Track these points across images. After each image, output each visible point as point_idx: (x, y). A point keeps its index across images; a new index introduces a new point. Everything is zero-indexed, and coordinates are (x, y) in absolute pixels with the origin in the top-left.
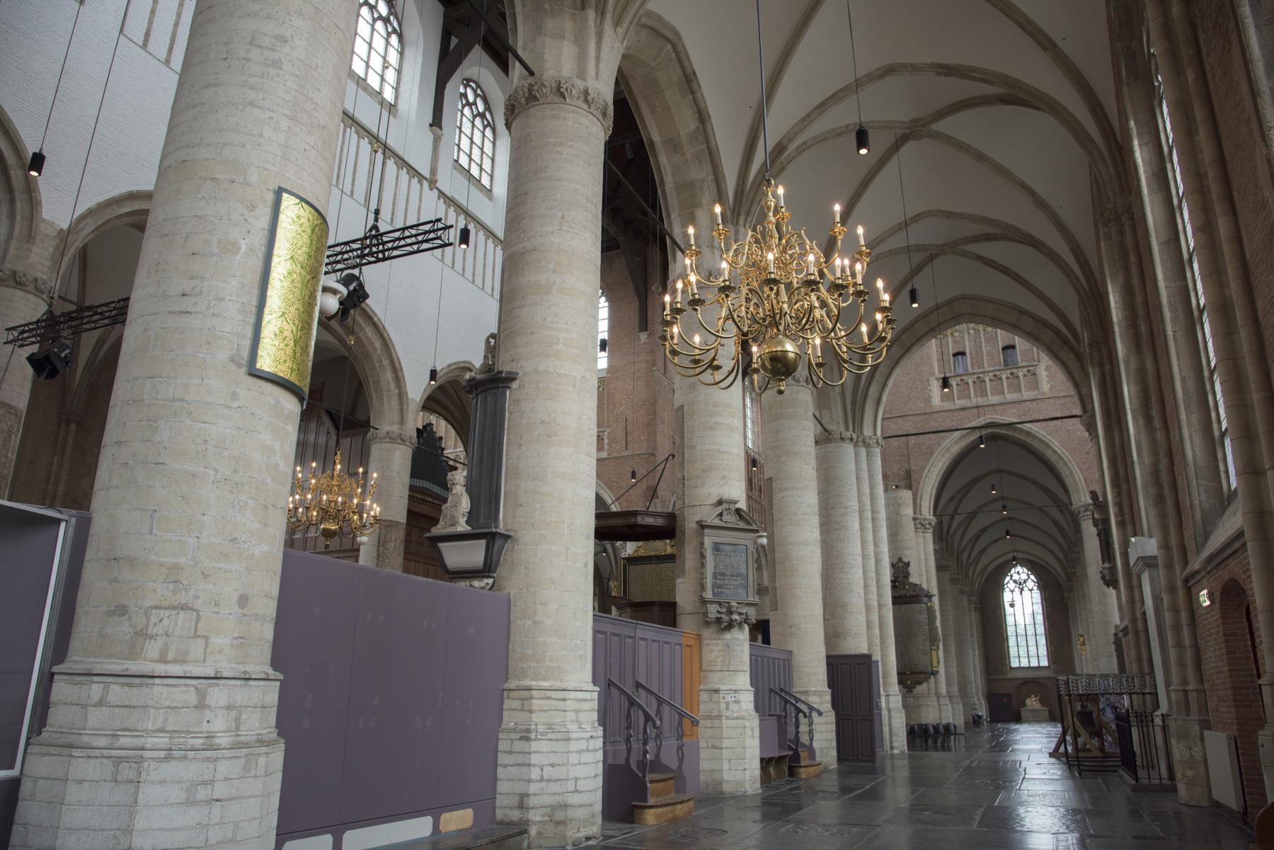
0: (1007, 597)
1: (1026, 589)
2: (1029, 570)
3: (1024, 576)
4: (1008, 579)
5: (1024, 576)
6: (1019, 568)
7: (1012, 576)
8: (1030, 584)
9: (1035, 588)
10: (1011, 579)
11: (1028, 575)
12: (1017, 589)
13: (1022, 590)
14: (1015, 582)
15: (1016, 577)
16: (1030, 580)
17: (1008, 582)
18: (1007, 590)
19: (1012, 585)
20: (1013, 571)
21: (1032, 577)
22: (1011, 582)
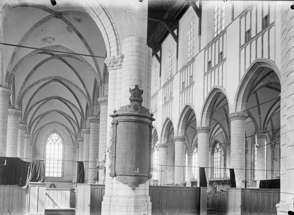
0: (48, 146)
1: (57, 143)
2: (59, 136)
4: (49, 138)
5: (57, 138)
6: (55, 135)
7: (51, 137)
8: (59, 142)
9: (61, 143)
11: (58, 138)
12: (53, 143)
13: (55, 144)
14: (52, 140)
16: (59, 140)
17: (49, 140)
18: (48, 143)
20: (52, 135)
21: (60, 139)
22: (51, 140)
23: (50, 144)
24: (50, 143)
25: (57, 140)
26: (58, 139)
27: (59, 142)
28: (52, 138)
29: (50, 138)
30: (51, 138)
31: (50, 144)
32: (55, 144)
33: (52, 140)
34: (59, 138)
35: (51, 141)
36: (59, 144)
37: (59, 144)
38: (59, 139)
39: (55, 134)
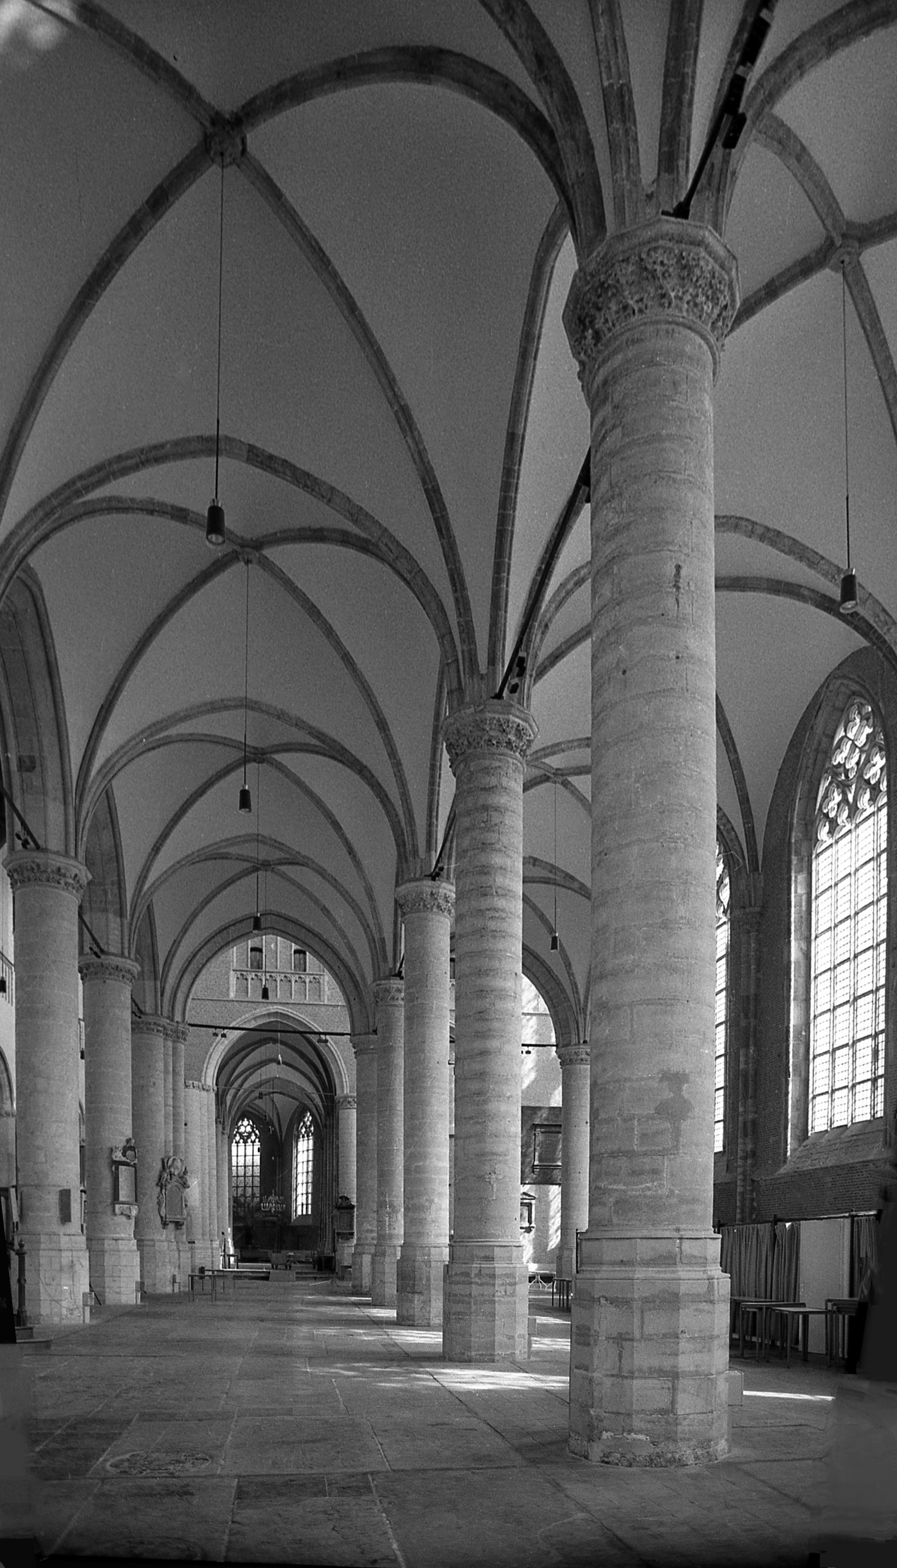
1: (249, 1140)
5: (249, 1129)
6: (246, 1123)
7: (238, 1128)
8: (253, 1137)
11: (252, 1127)
12: (241, 1141)
13: (245, 1142)
14: (241, 1134)
15: (242, 1129)
19: (238, 1138)
20: (240, 1123)
21: (257, 1132)
23: (237, 1143)
25: (250, 1134)
27: (253, 1137)
32: (245, 1142)
33: (241, 1134)
35: (238, 1138)
36: (253, 1142)
37: (253, 1142)
38: (253, 1131)
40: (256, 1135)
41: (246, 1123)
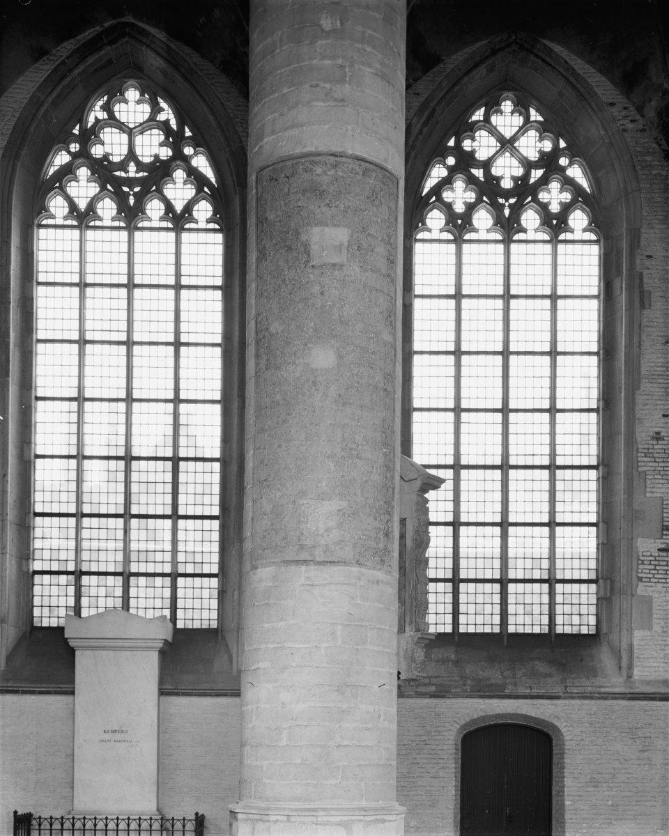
1: (154, 208)
3: (151, 146)
5: (151, 146)
9: (204, 210)
10: (83, 155)
11: (174, 139)
12: (108, 208)
13: (131, 216)
14: (104, 171)
15: (112, 145)
16: (179, 175)
17: (67, 172)
18: (57, 205)
19: (83, 188)
20: (97, 113)
22: (83, 172)
24: (73, 206)
25: (159, 173)
26: (165, 153)
27: (179, 191)
28: (97, 151)
29: (74, 147)
30: (83, 155)
31: (83, 218)
32: (131, 216)
33: (104, 171)
34: (188, 151)
37: (179, 220)
39: (132, 94)
40: (195, 176)
41: (133, 107)
